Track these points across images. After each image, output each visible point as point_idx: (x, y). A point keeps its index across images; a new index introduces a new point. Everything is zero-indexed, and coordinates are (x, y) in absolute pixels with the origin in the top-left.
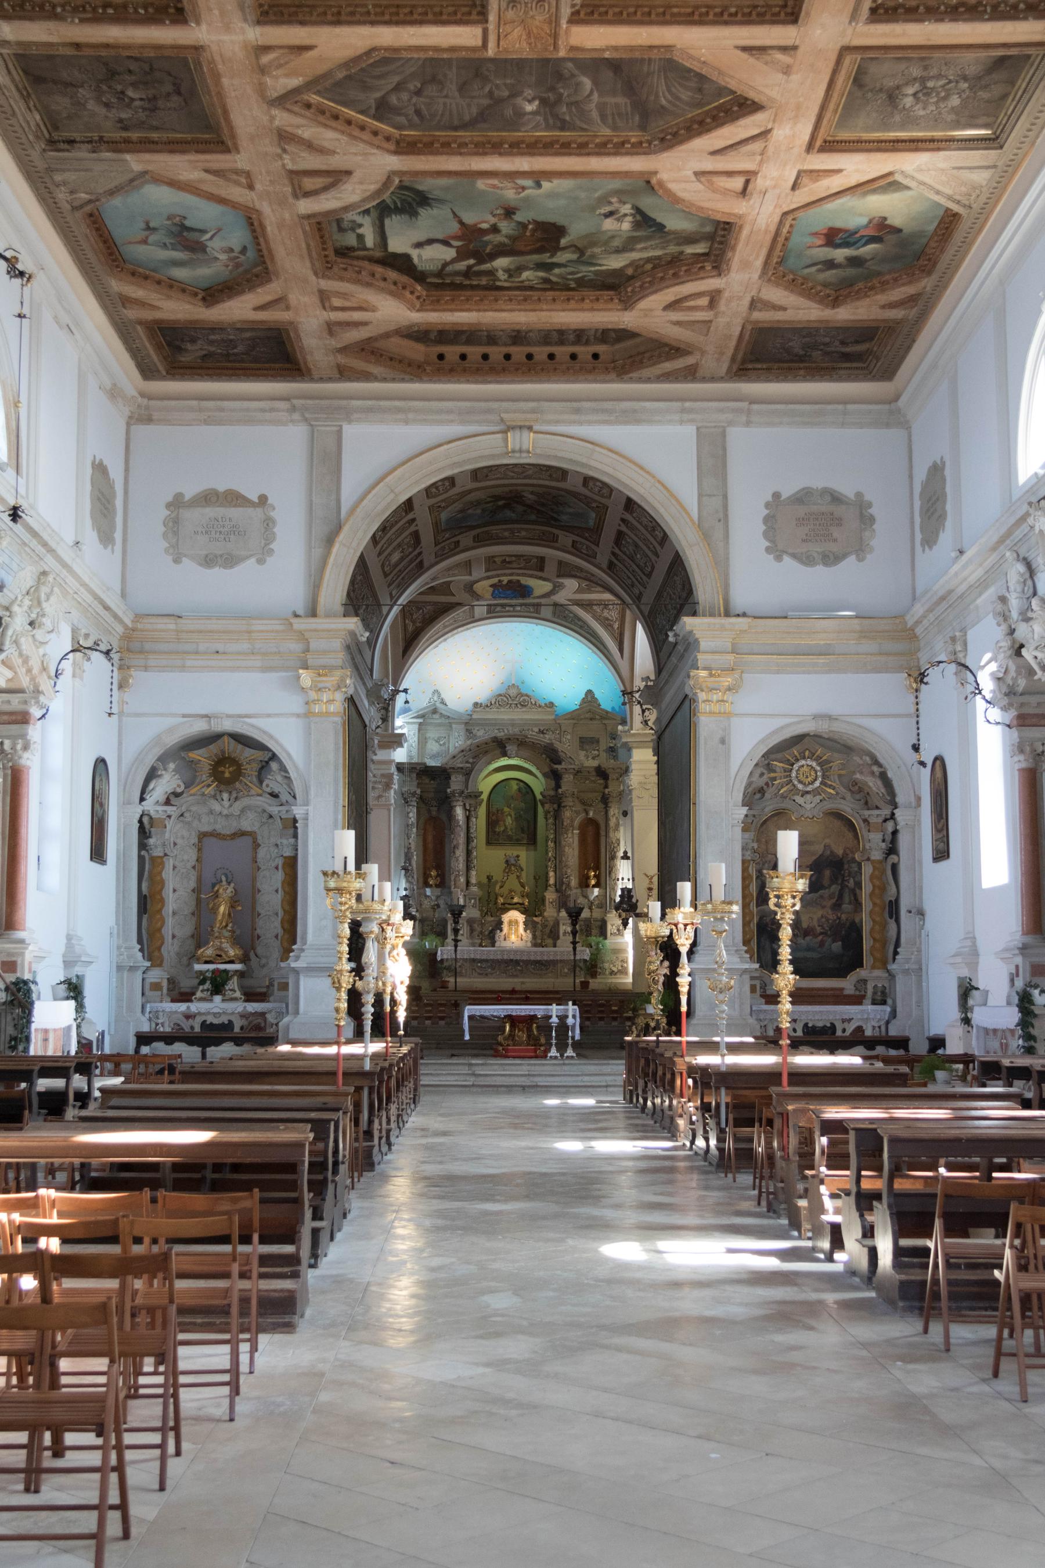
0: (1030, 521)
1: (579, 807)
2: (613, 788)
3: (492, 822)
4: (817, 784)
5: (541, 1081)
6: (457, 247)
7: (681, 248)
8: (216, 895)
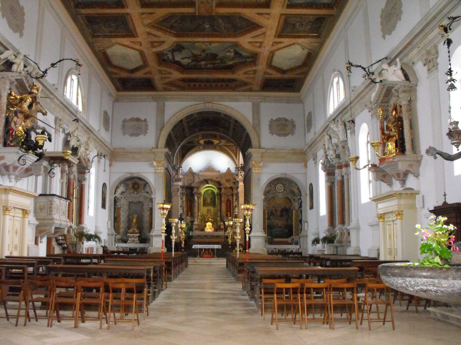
0: (329, 125)
1: (226, 196)
2: (235, 192)
3: (205, 200)
4: (282, 190)
5: (213, 263)
7: (247, 60)
8: (133, 217)
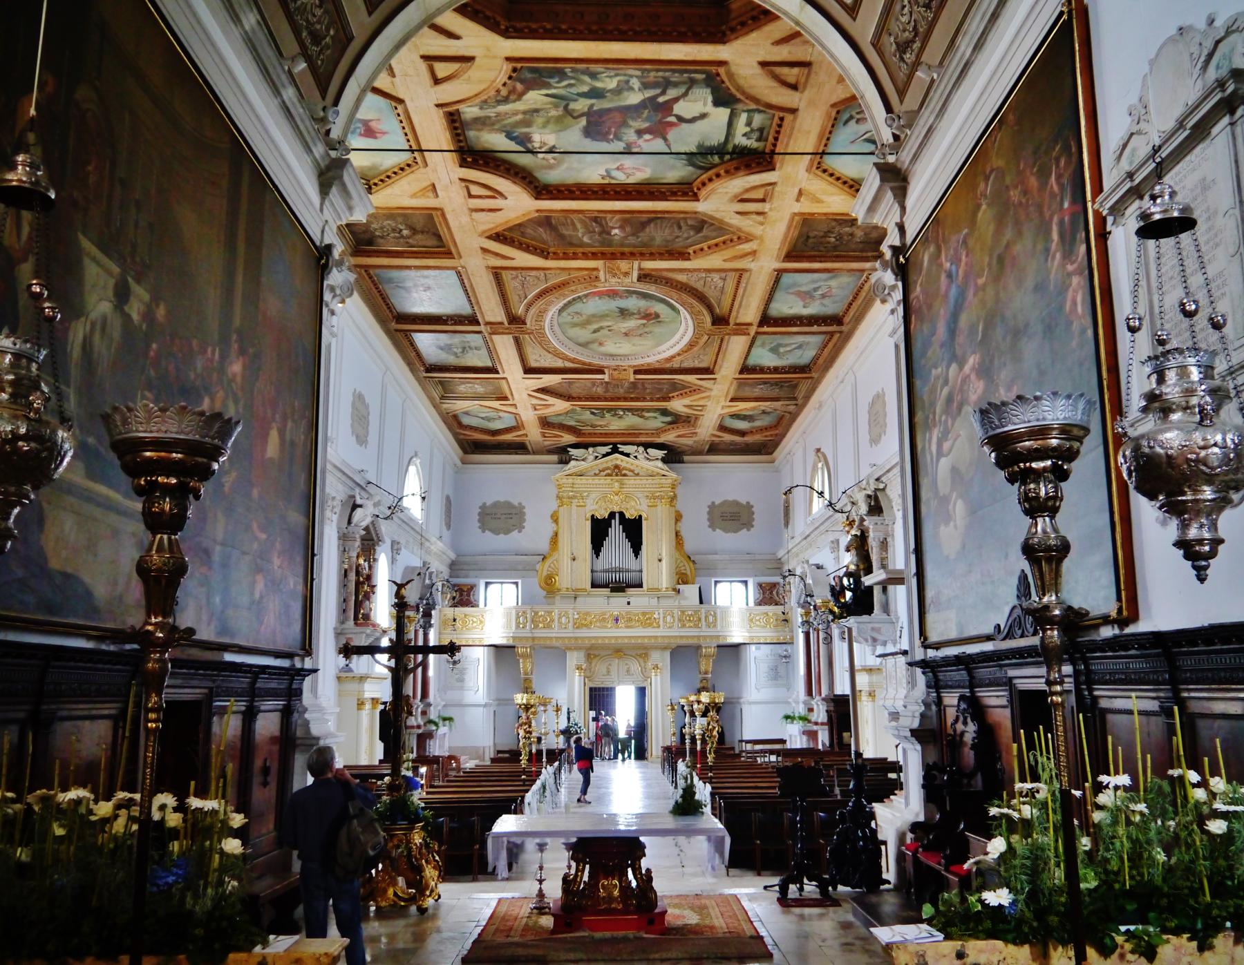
6: (671, 115)
